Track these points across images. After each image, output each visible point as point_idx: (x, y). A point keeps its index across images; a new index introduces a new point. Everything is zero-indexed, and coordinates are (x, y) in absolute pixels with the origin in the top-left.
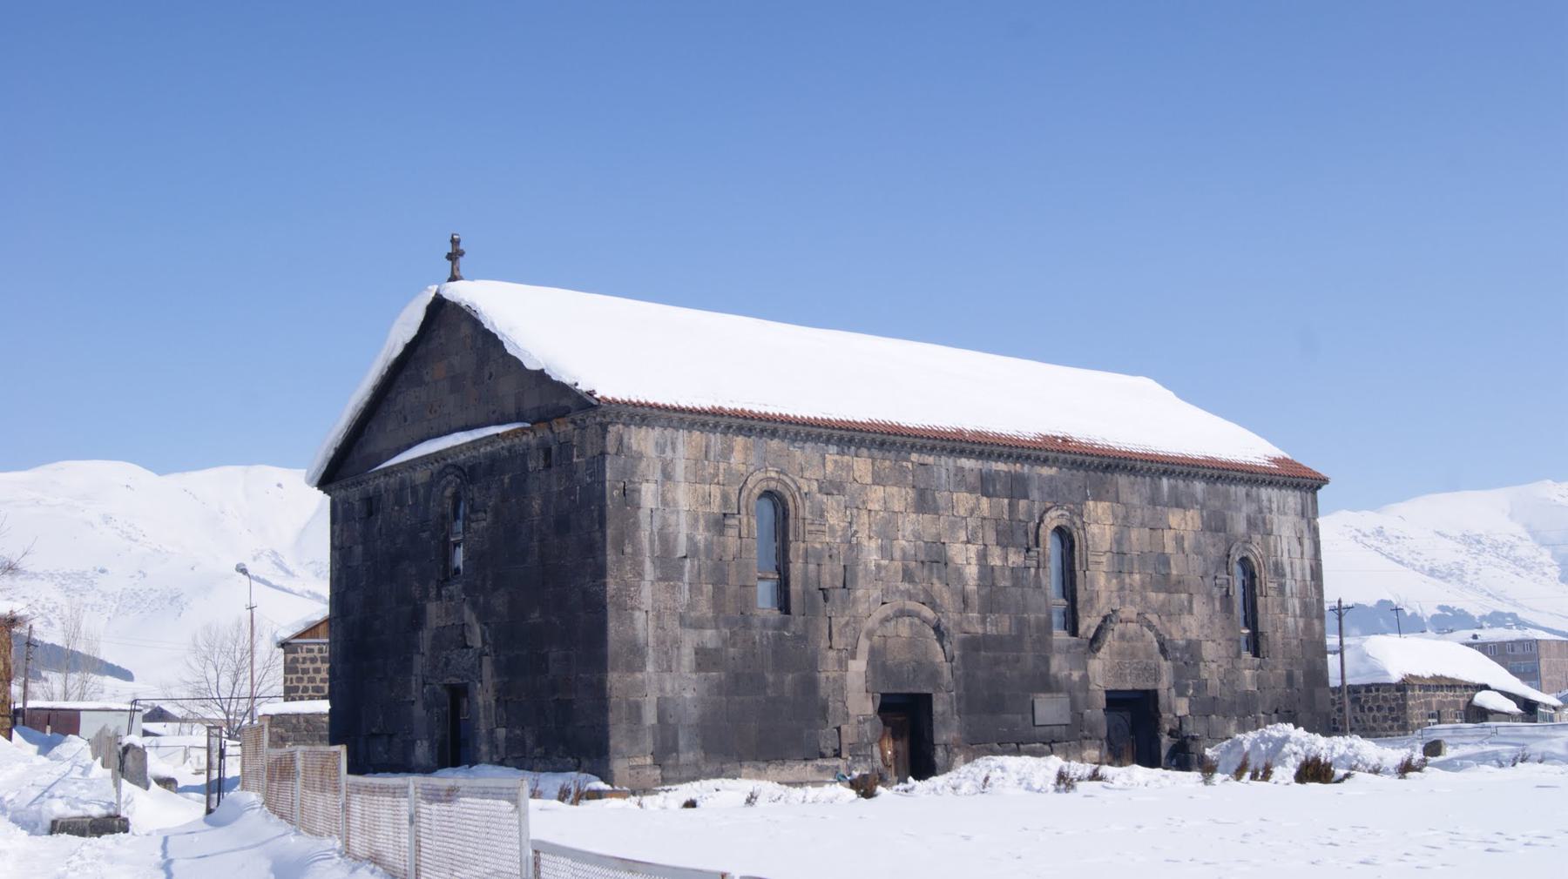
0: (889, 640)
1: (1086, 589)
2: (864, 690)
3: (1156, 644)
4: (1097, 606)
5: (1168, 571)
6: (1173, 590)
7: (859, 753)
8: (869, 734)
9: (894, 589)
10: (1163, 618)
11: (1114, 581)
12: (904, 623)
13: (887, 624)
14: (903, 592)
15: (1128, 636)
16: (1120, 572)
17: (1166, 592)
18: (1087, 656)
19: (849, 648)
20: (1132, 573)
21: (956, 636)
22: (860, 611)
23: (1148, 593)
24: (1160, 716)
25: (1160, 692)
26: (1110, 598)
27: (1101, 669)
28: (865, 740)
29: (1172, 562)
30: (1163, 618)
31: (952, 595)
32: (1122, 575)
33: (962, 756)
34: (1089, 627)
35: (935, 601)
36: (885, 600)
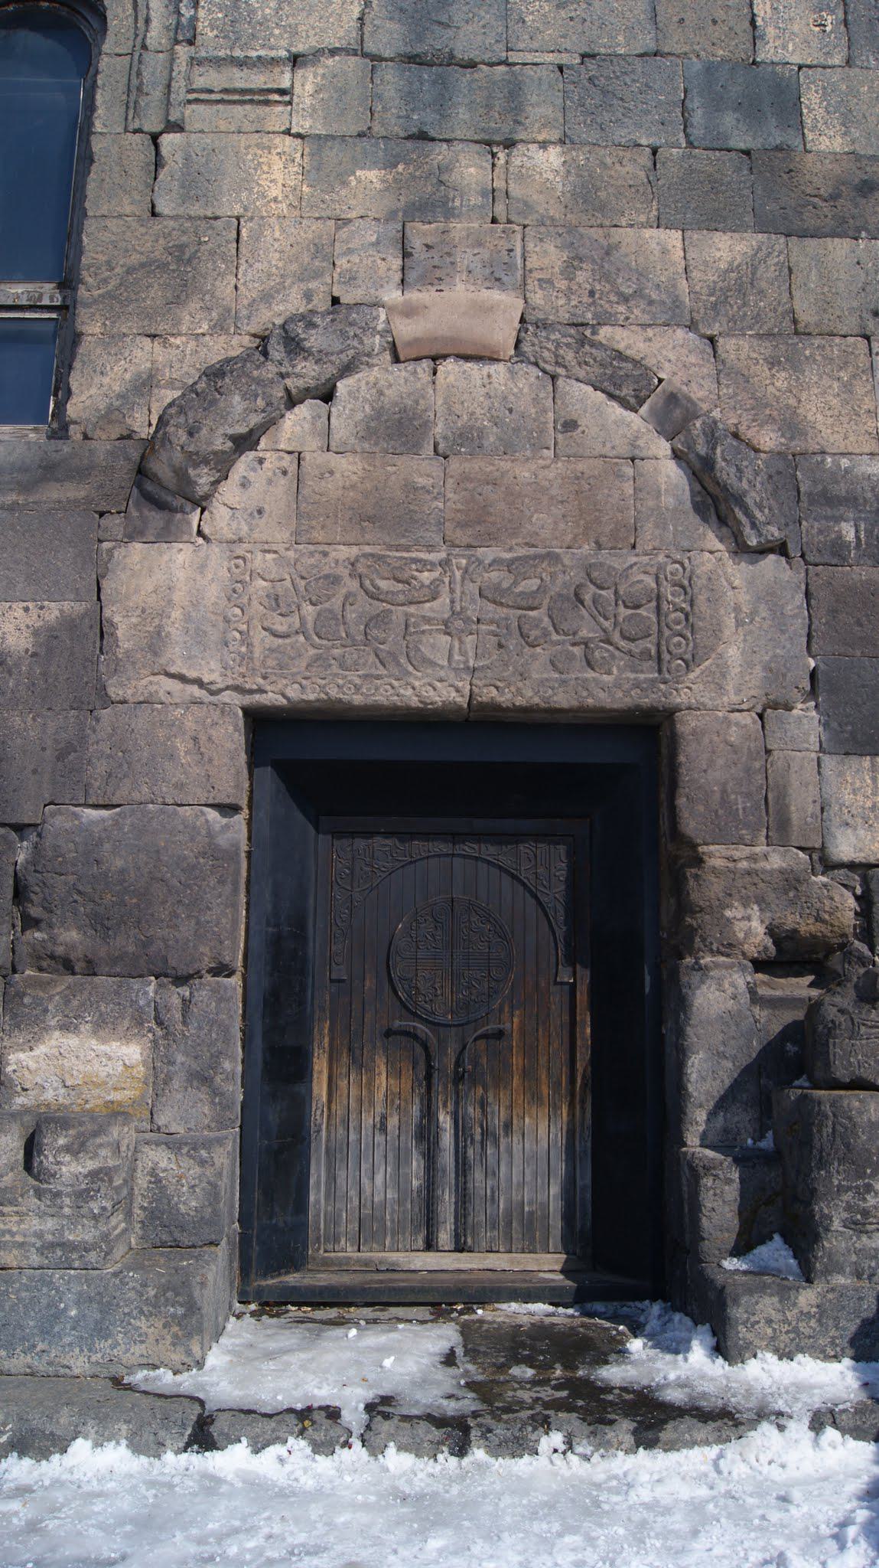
1: (154, 214)
3: (670, 474)
4: (224, 289)
5: (777, 137)
6: (811, 221)
10: (735, 348)
11: (372, 176)
15: (439, 429)
16: (423, 136)
17: (763, 226)
18: (114, 524)
20: (509, 144)
23: (625, 236)
24: (698, 861)
25: (687, 724)
26: (324, 253)
27: (213, 593)
29: (811, 99)
30: (735, 348)
32: (440, 153)
34: (146, 384)
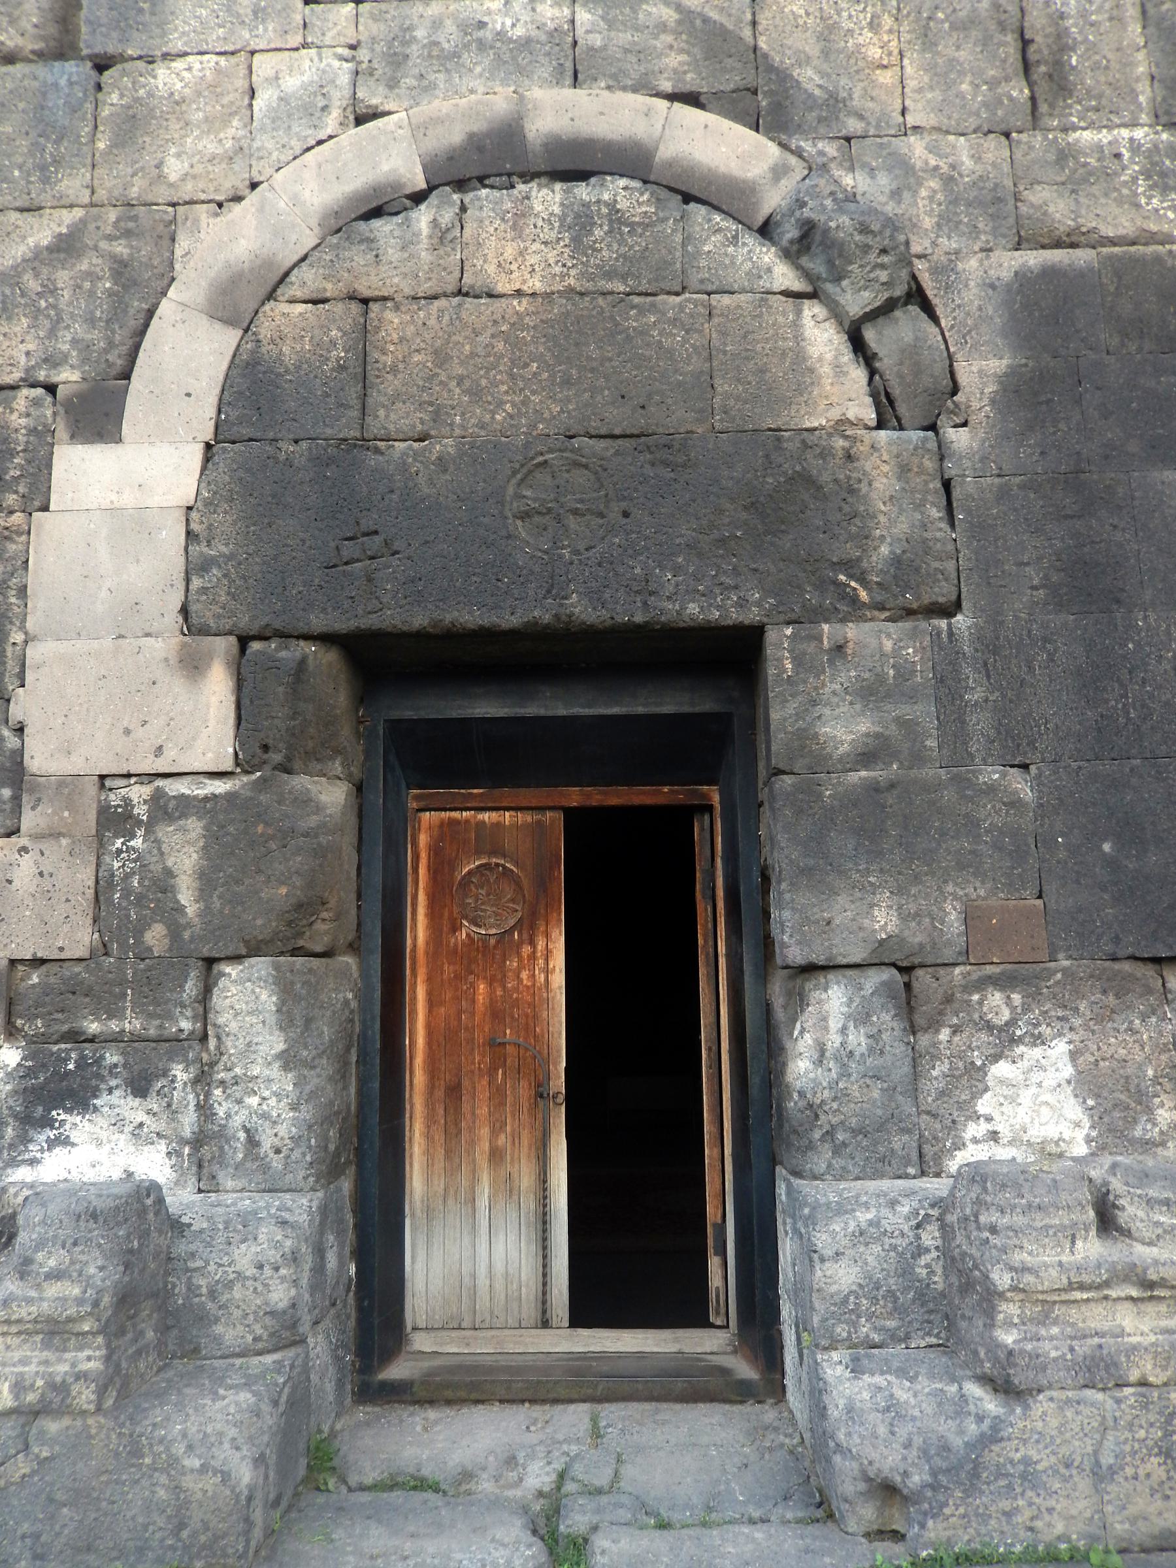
0: (392, 322)
2: (173, 619)
7: (93, 1027)
8: (187, 896)
9: (449, 36)
12: (519, 220)
13: (382, 227)
14: (526, 43)
19: (68, 377)
21: (971, 265)
22: (174, 168)
28: (156, 936)
31: (926, 38)
33: (1060, 1048)
35: (783, 77)
36: (371, 94)
